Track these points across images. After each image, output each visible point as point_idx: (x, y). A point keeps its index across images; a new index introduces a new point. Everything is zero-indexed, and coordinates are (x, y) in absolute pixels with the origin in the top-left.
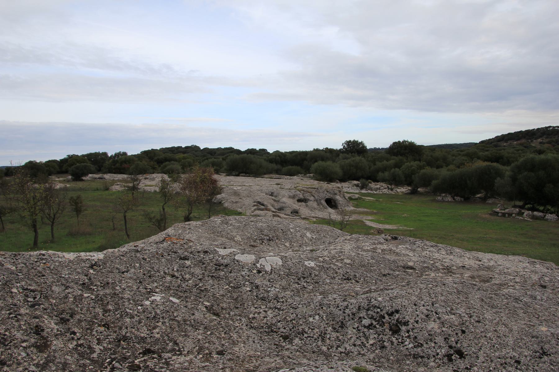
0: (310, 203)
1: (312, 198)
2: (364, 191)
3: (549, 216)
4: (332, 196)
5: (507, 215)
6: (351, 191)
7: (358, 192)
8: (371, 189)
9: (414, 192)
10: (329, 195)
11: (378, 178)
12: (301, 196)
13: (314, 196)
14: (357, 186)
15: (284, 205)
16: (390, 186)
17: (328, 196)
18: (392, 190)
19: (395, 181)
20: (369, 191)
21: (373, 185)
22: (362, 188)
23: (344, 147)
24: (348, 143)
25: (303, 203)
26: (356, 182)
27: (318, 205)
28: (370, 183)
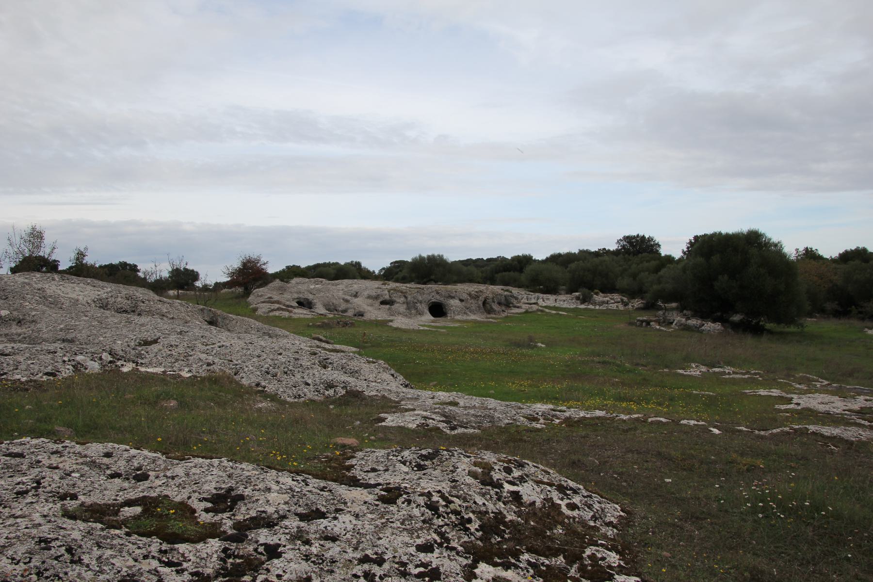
0: (396, 306)
1: (403, 299)
2: (583, 306)
3: (710, 326)
4: (442, 299)
5: (644, 324)
6: (565, 305)
7: (573, 306)
8: (595, 304)
9: (650, 307)
10: (438, 297)
11: (617, 287)
12: (387, 297)
13: (406, 297)
14: (578, 298)
15: (349, 305)
16: (625, 299)
17: (437, 298)
18: (626, 304)
19: (632, 293)
20: (591, 307)
21: (599, 297)
22: (583, 301)
23: (623, 247)
24: (628, 239)
25: (388, 306)
26: (577, 294)
27: (408, 308)
28: (597, 294)
